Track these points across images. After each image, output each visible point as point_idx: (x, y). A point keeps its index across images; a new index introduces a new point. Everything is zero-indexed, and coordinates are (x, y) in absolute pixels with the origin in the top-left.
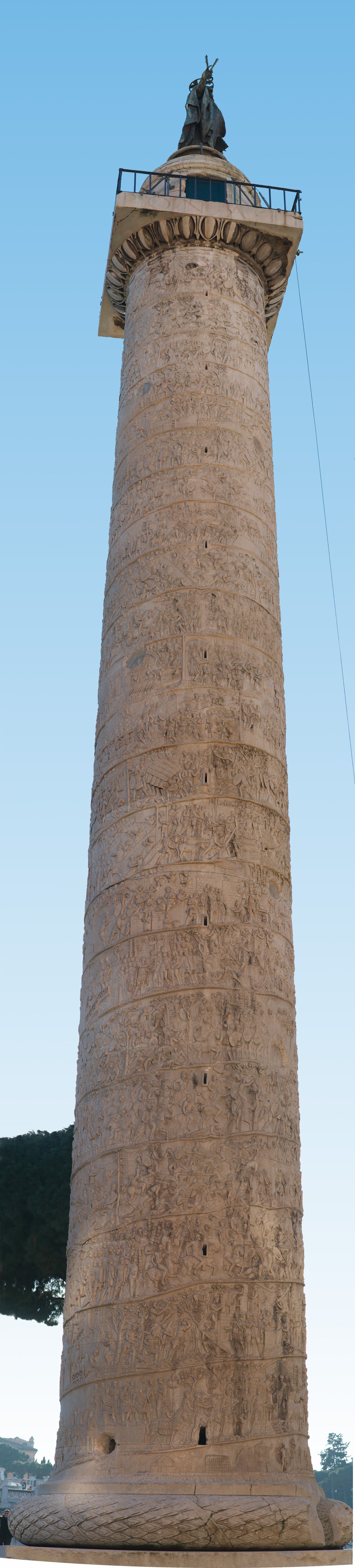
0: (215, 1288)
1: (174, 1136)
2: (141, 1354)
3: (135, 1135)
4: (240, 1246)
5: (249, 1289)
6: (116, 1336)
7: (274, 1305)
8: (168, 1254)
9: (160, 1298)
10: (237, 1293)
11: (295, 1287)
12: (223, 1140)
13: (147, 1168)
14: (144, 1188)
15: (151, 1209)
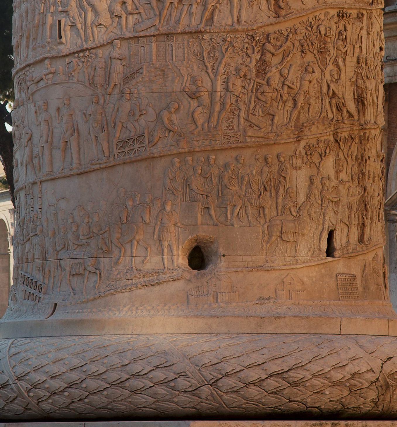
0: (342, 15)
2: (252, 114)
6: (210, 84)
9: (277, 28)
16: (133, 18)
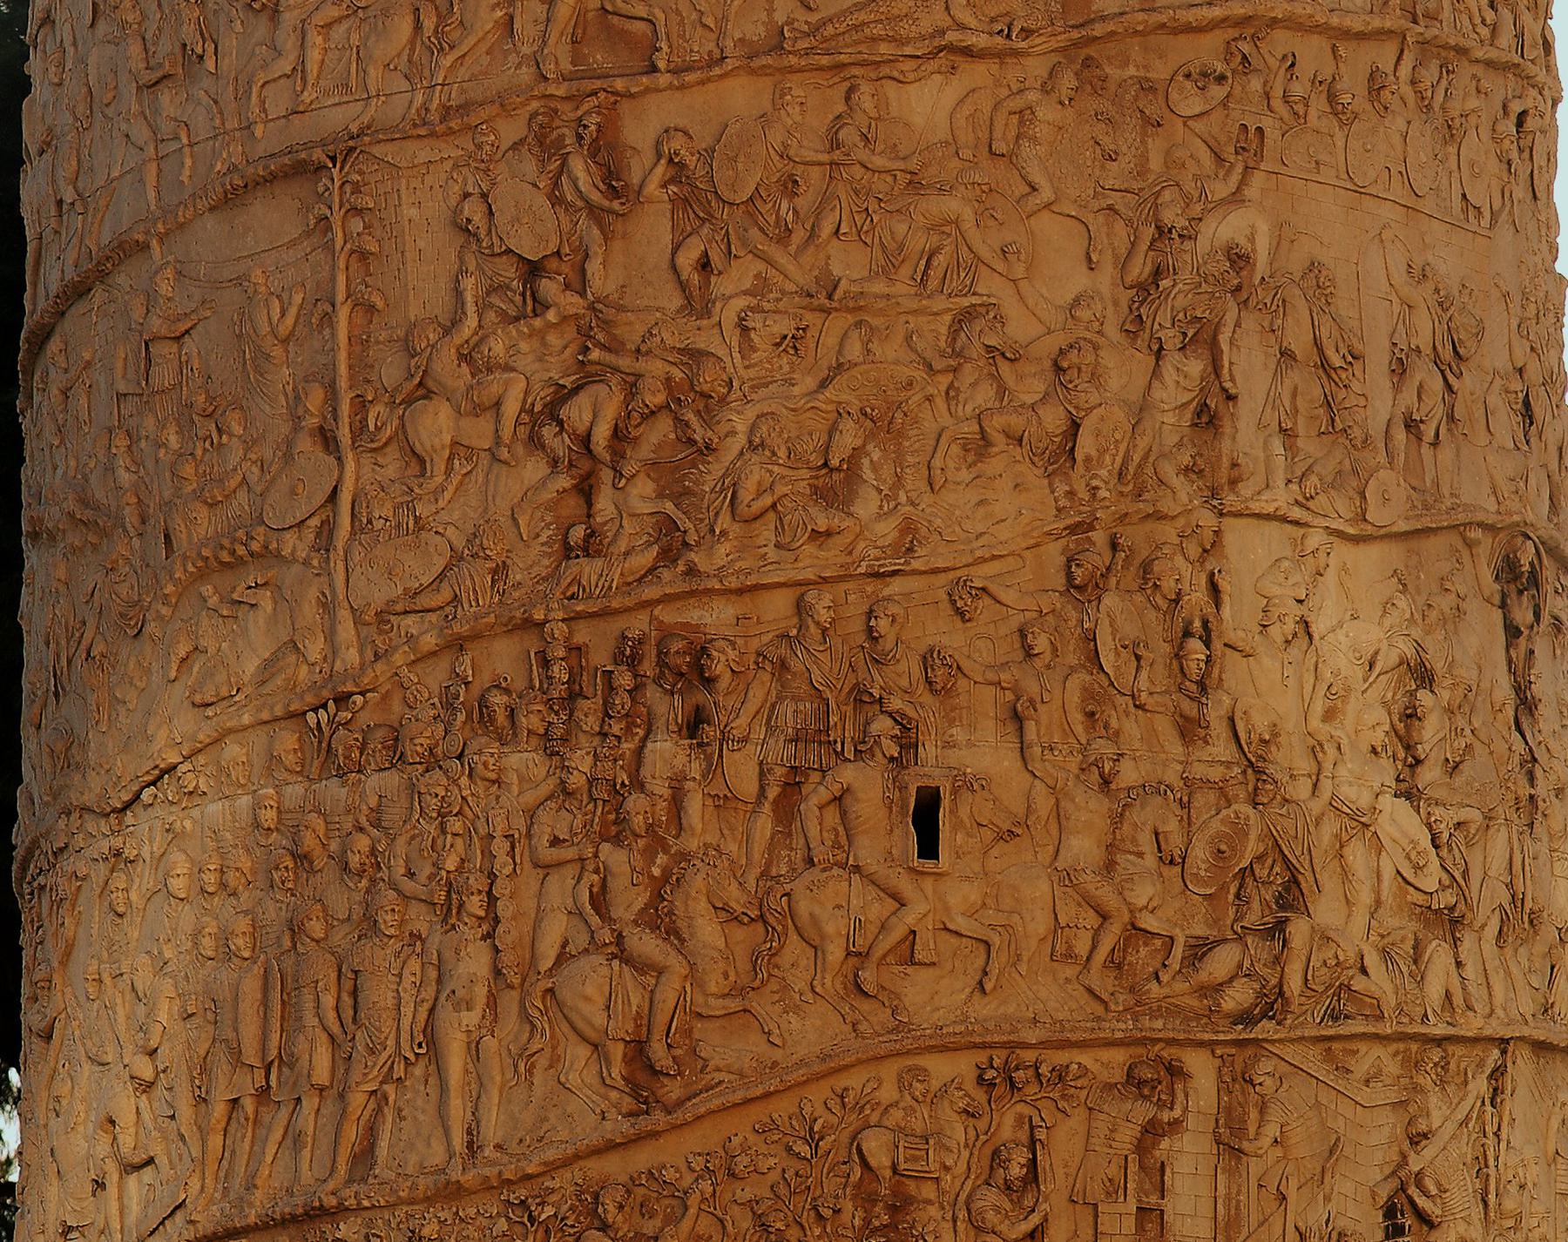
1: (702, 45)
3: (441, 44)
4: (1159, 789)
5: (1223, 1087)
7: (1383, 1196)
8: (684, 856)
9: (642, 1159)
10: (1143, 1112)
11: (1522, 1066)
12: (1037, 68)
13: (533, 270)
14: (511, 408)
15: (567, 552)
16: (140, 1181)
